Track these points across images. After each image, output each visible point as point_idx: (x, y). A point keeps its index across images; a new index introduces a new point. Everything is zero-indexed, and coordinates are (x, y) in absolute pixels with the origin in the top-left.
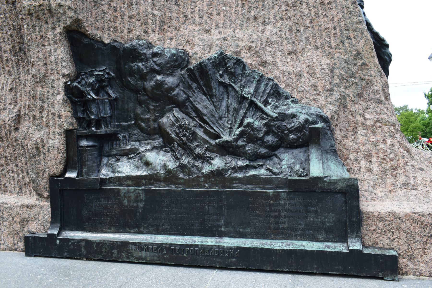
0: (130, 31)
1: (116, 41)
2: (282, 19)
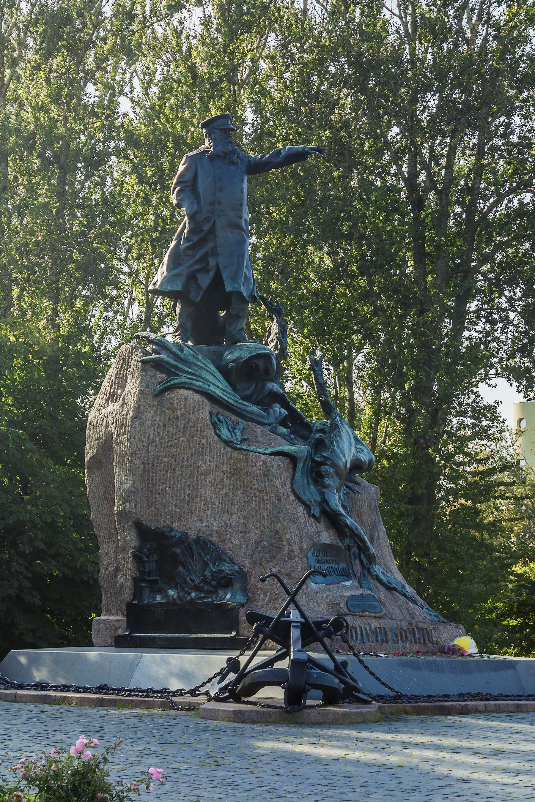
0: (164, 522)
1: (157, 528)
2: (241, 511)
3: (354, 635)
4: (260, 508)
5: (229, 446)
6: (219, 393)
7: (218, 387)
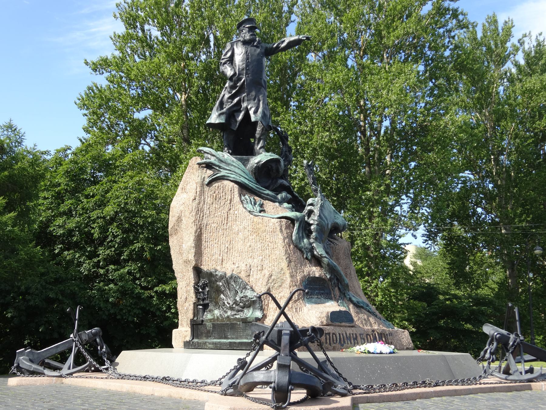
3: (335, 339)
4: (271, 253)
5: (252, 214)
6: (247, 182)
7: (246, 178)
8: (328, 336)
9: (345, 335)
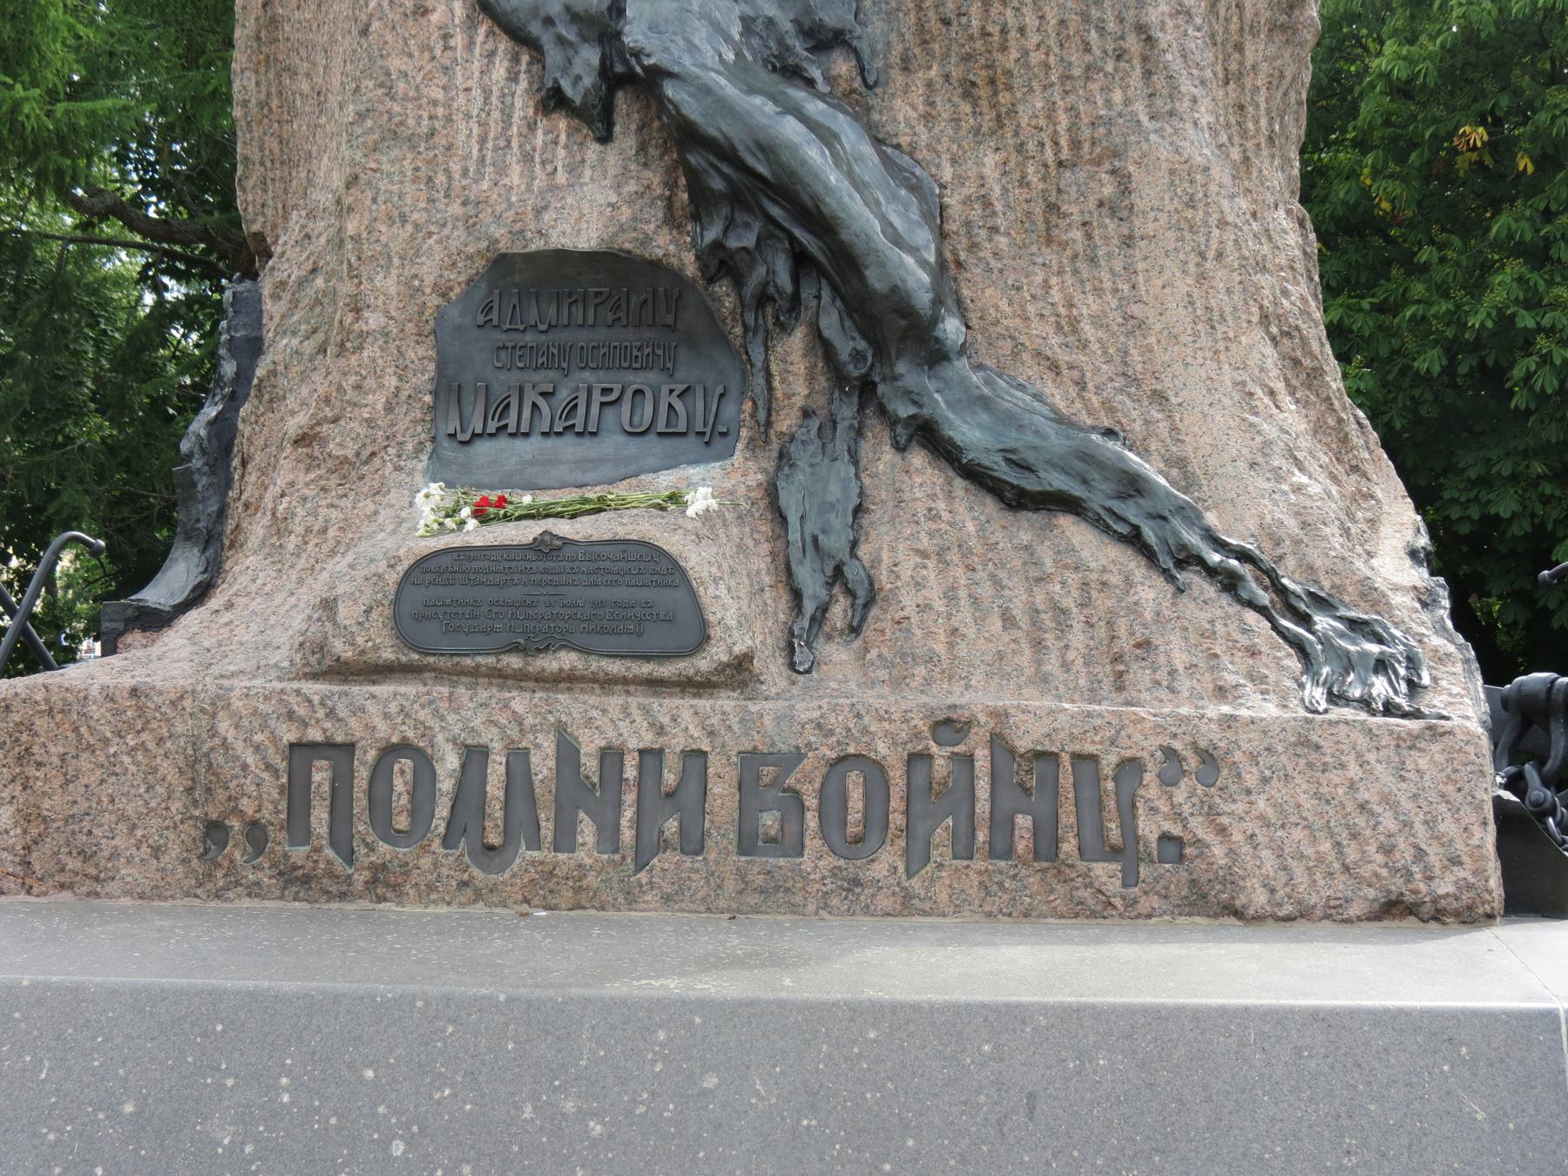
8: (321, 776)
9: (543, 764)
